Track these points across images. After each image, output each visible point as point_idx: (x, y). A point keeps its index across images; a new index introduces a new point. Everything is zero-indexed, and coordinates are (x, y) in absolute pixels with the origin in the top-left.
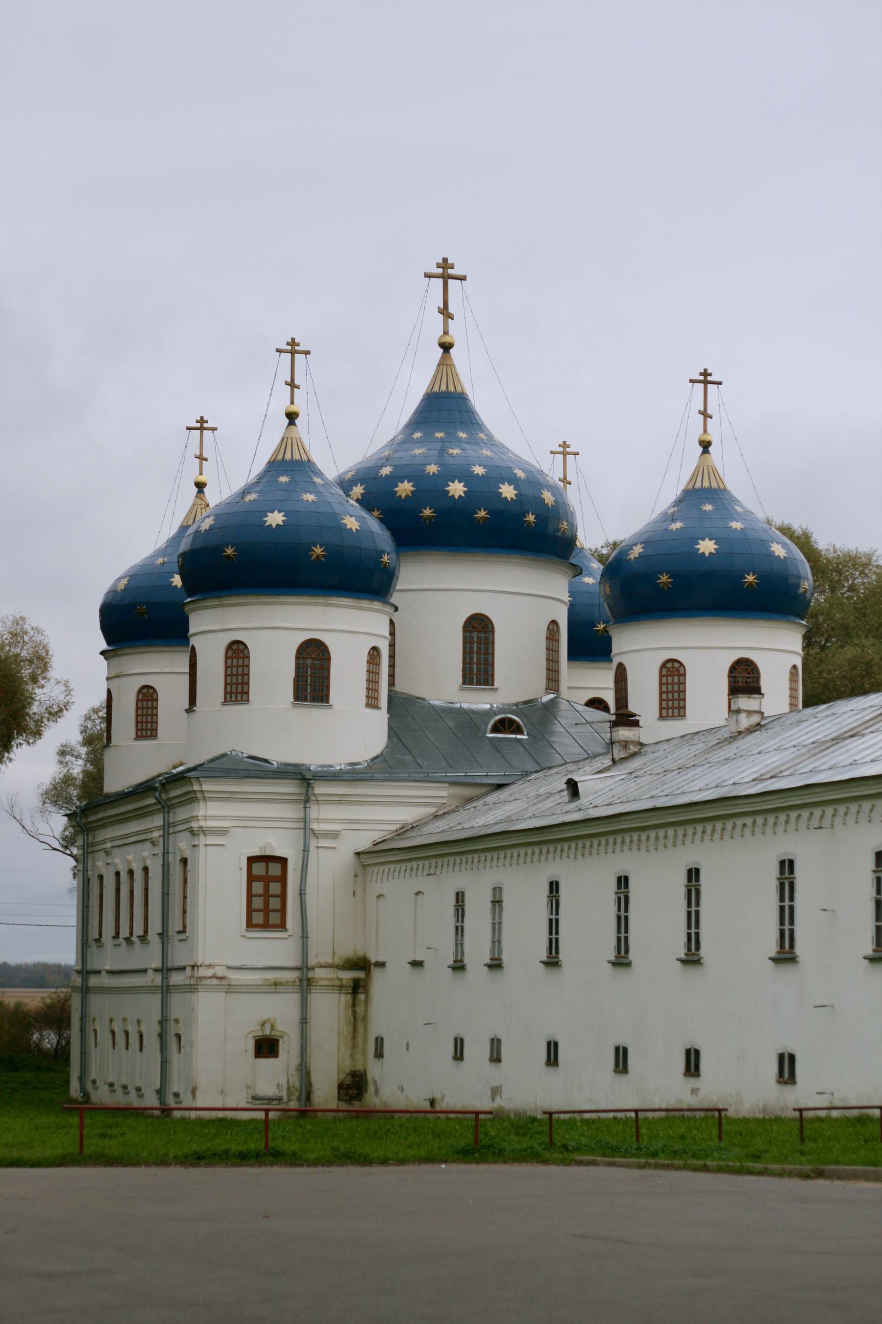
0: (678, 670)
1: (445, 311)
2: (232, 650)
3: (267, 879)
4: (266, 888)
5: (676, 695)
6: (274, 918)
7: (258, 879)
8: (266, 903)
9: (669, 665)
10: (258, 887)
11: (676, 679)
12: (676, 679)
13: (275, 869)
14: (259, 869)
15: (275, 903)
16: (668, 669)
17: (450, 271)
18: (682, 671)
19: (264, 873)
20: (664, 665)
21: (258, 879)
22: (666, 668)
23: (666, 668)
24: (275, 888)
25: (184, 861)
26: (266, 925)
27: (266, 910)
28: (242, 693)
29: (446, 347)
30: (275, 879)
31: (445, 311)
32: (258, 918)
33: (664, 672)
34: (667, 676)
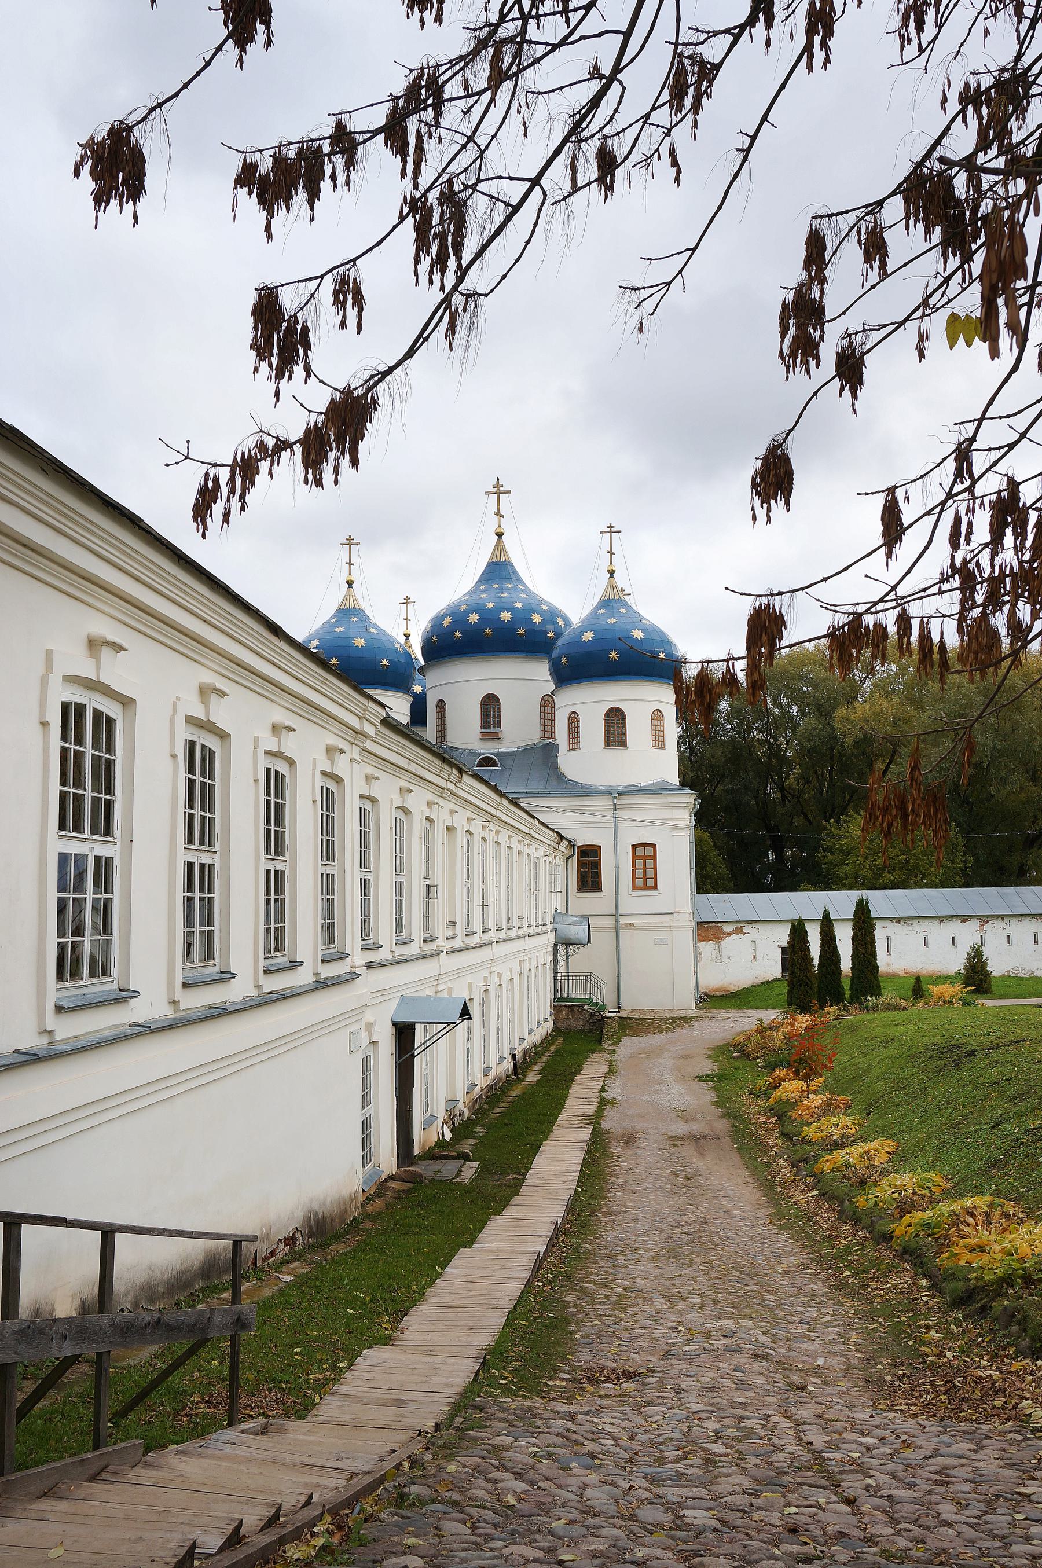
1: (498, 514)
3: (645, 858)
4: (645, 864)
6: (650, 883)
7: (640, 858)
8: (645, 873)
10: (639, 863)
13: (649, 852)
14: (639, 852)
15: (650, 873)
17: (501, 489)
21: (640, 858)
24: (650, 863)
26: (645, 887)
27: (645, 878)
29: (500, 535)
30: (650, 858)
31: (498, 514)
32: (640, 883)
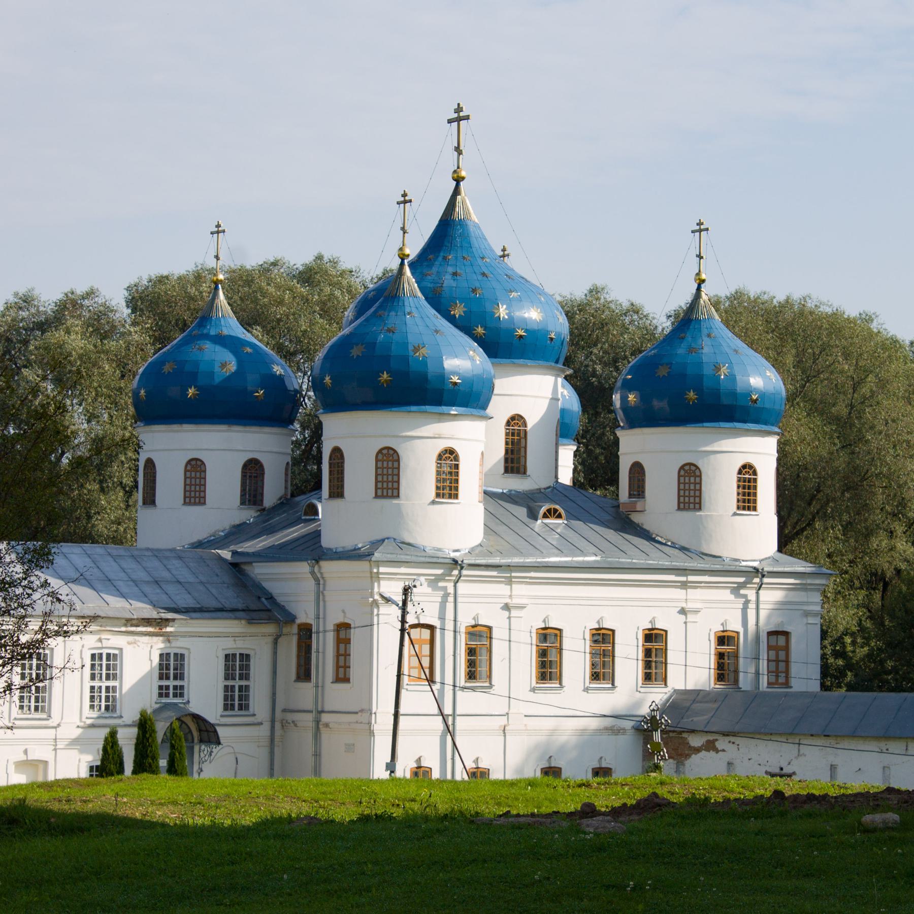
0: (694, 472)
2: (382, 454)
3: (421, 642)
5: (692, 493)
9: (687, 468)
11: (692, 480)
12: (692, 480)
16: (686, 471)
18: (697, 473)
19: (419, 637)
20: (682, 468)
22: (684, 470)
23: (684, 470)
25: (343, 628)
28: (393, 489)
33: (682, 473)
34: (684, 476)
